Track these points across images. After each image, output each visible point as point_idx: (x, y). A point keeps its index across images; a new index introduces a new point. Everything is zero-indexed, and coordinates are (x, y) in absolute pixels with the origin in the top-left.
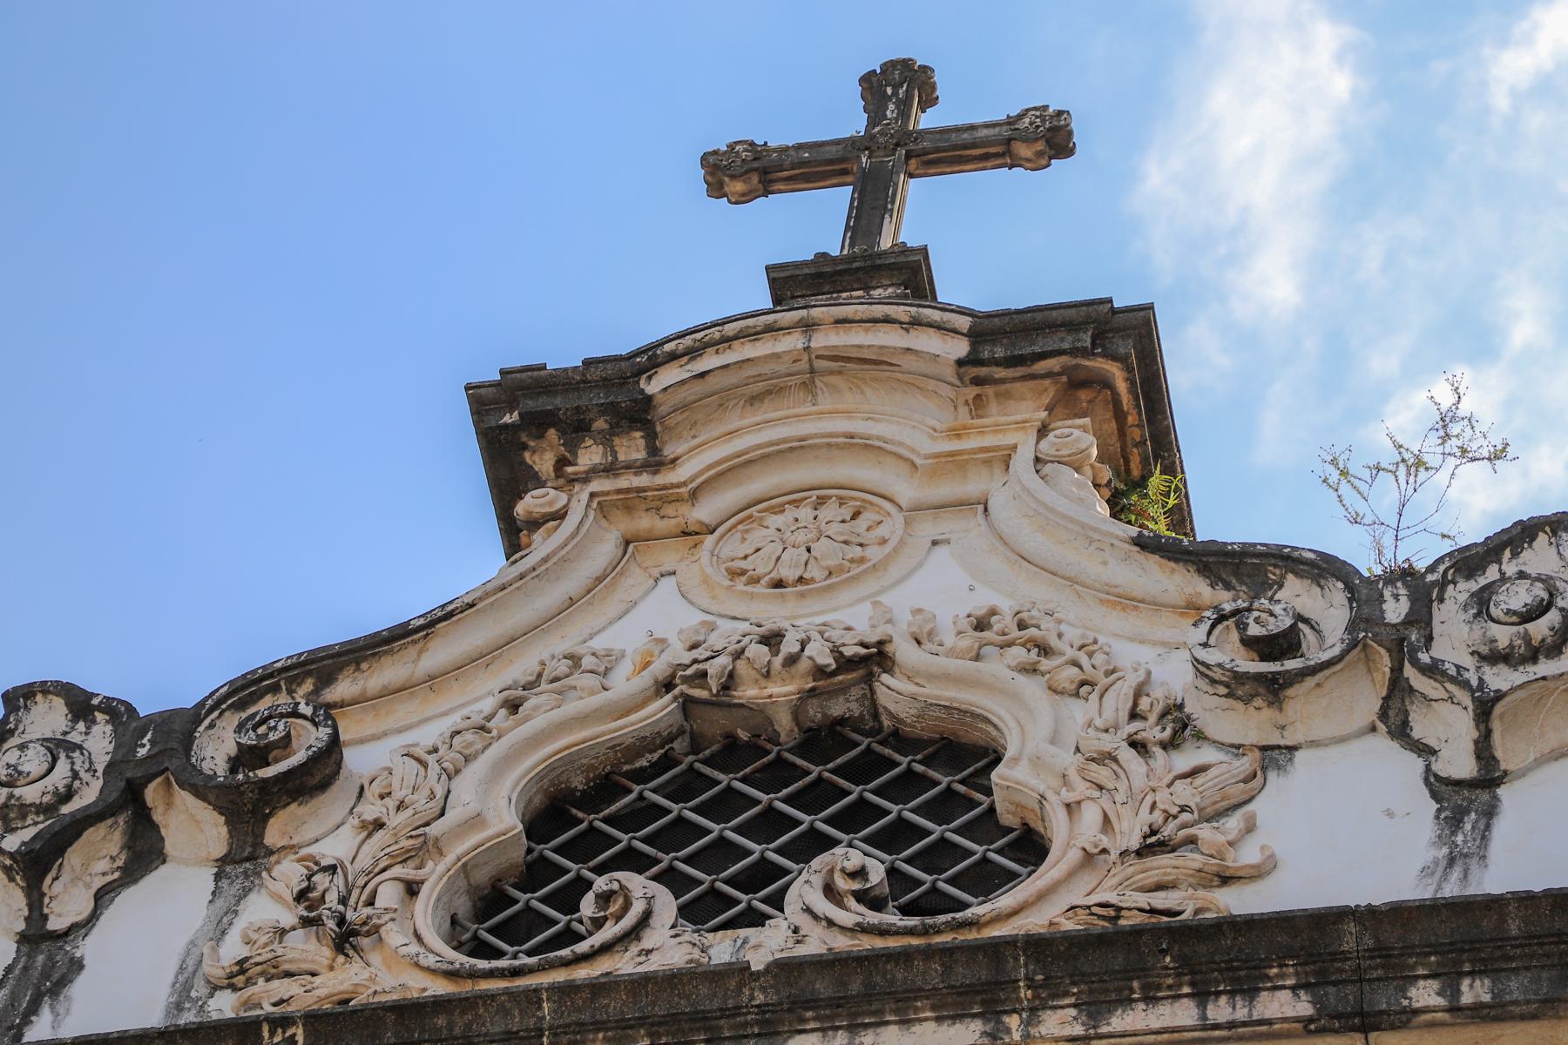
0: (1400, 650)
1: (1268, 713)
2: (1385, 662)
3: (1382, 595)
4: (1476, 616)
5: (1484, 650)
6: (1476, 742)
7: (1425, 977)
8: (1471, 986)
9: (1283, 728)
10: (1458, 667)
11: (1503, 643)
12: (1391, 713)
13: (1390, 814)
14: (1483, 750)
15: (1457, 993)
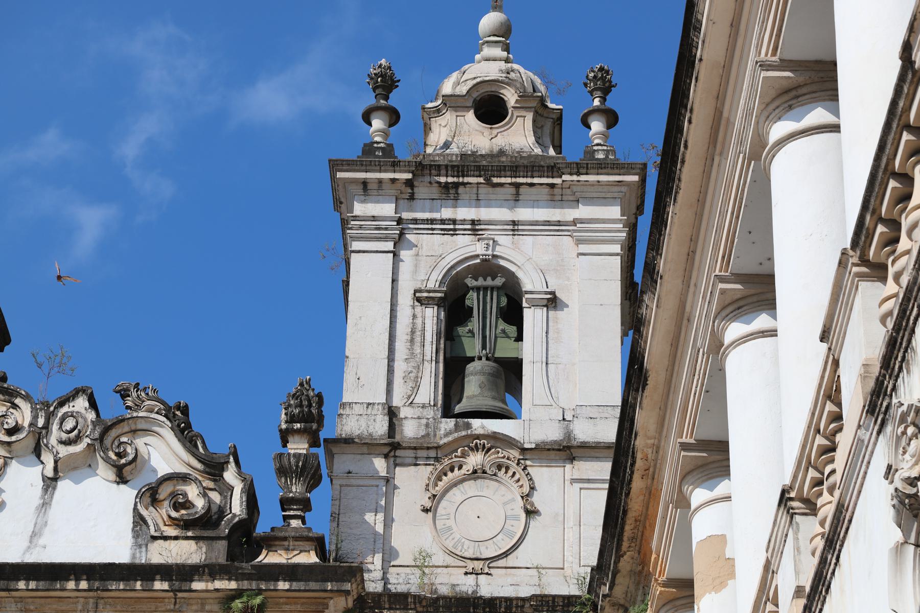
0: (40, 434)
1: (7, 448)
2: (37, 436)
3: (38, 415)
4: (59, 428)
5: (60, 440)
6: (54, 467)
7: (23, 579)
8: (32, 583)
9: (10, 452)
10: (52, 446)
11: (64, 439)
12: (37, 449)
13: (32, 486)
14: (56, 469)
15: (28, 585)
